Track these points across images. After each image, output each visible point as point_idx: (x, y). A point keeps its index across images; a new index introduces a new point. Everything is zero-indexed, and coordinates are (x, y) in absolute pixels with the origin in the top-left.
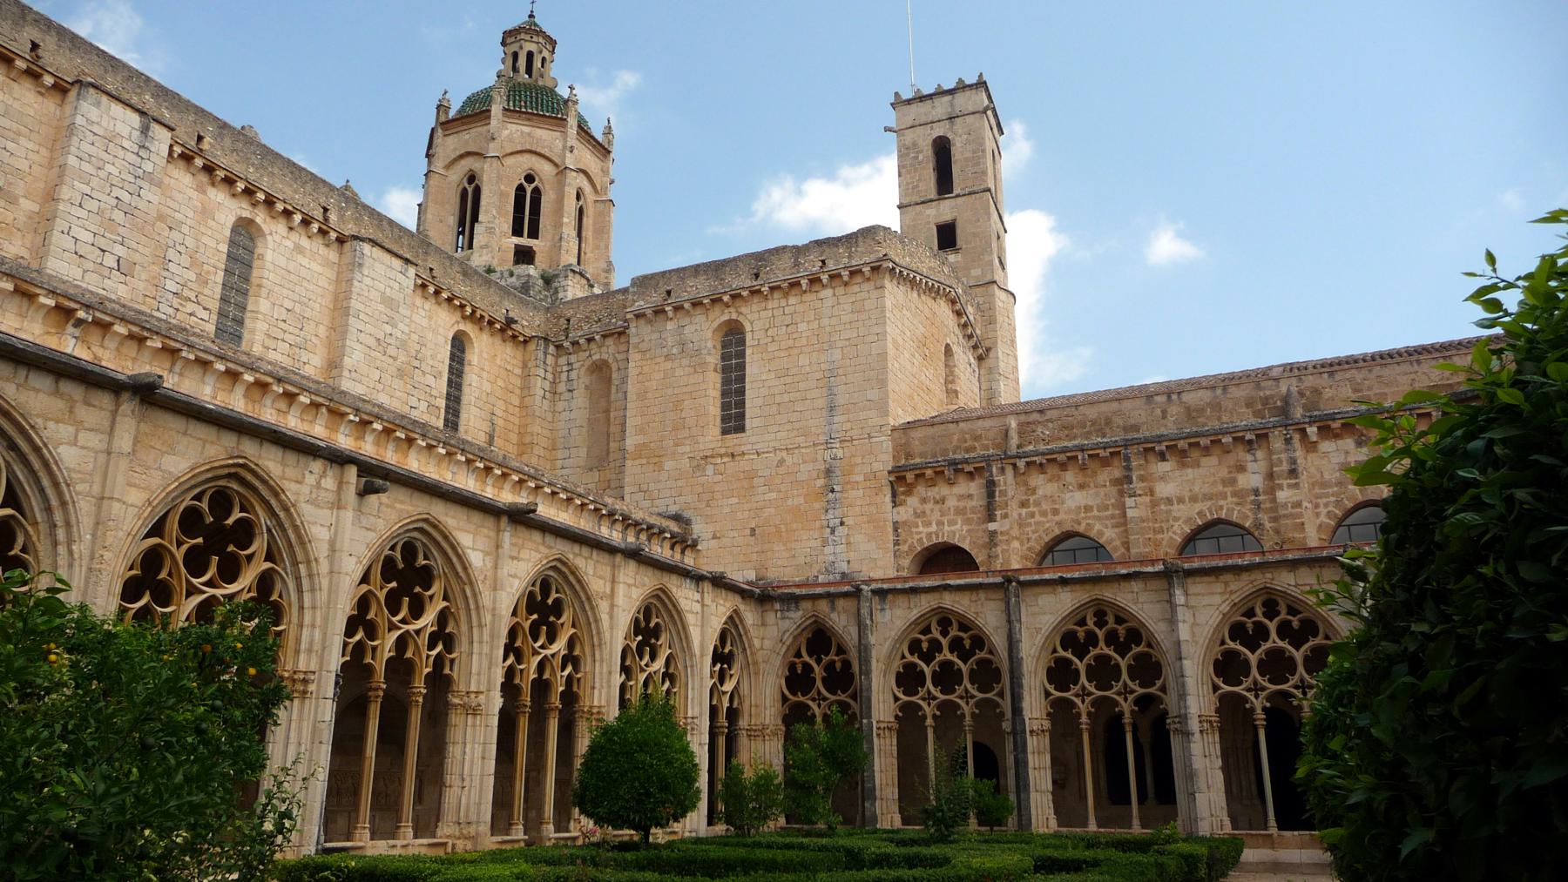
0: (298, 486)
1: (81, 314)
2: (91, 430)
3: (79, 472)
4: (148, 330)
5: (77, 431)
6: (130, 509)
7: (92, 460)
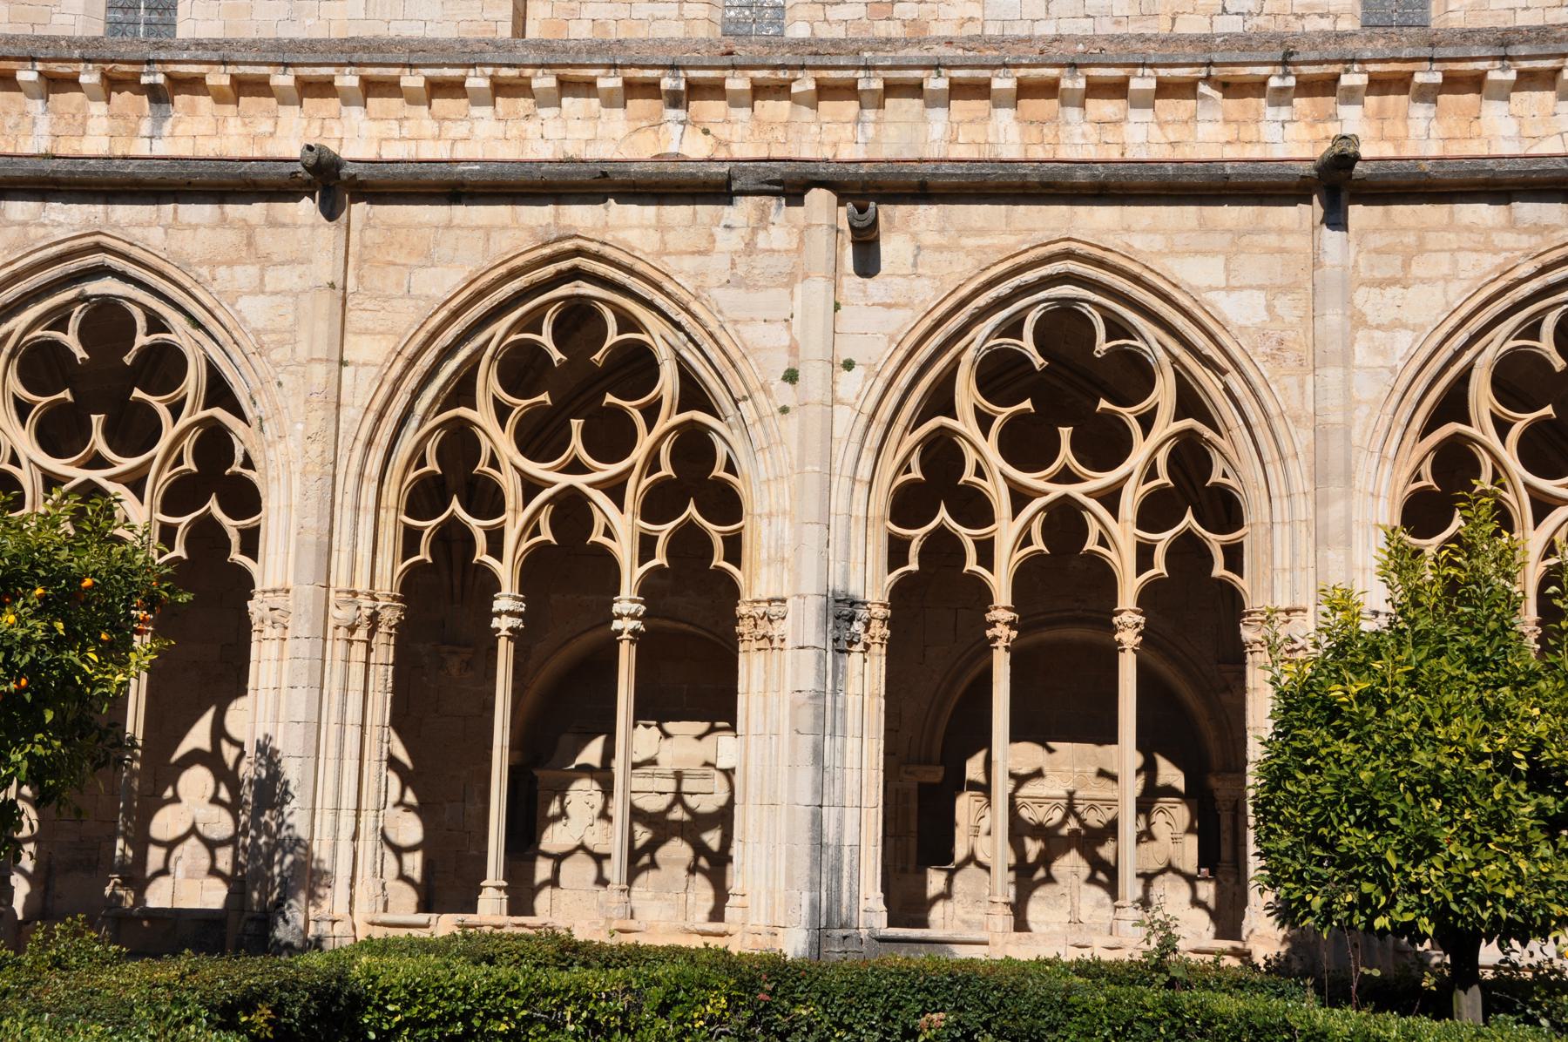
0: (699, 259)
1: (667, 83)
2: (282, 264)
3: (273, 331)
4: (783, 67)
5: (263, 269)
6: (362, 371)
7: (291, 308)
